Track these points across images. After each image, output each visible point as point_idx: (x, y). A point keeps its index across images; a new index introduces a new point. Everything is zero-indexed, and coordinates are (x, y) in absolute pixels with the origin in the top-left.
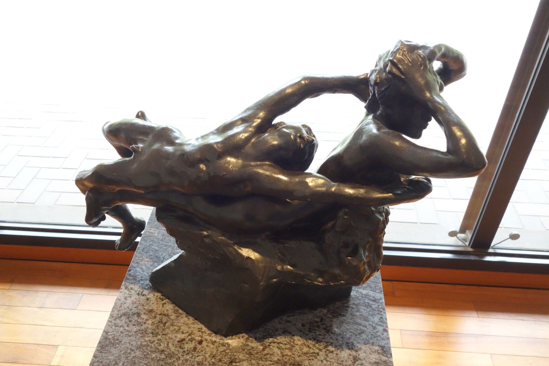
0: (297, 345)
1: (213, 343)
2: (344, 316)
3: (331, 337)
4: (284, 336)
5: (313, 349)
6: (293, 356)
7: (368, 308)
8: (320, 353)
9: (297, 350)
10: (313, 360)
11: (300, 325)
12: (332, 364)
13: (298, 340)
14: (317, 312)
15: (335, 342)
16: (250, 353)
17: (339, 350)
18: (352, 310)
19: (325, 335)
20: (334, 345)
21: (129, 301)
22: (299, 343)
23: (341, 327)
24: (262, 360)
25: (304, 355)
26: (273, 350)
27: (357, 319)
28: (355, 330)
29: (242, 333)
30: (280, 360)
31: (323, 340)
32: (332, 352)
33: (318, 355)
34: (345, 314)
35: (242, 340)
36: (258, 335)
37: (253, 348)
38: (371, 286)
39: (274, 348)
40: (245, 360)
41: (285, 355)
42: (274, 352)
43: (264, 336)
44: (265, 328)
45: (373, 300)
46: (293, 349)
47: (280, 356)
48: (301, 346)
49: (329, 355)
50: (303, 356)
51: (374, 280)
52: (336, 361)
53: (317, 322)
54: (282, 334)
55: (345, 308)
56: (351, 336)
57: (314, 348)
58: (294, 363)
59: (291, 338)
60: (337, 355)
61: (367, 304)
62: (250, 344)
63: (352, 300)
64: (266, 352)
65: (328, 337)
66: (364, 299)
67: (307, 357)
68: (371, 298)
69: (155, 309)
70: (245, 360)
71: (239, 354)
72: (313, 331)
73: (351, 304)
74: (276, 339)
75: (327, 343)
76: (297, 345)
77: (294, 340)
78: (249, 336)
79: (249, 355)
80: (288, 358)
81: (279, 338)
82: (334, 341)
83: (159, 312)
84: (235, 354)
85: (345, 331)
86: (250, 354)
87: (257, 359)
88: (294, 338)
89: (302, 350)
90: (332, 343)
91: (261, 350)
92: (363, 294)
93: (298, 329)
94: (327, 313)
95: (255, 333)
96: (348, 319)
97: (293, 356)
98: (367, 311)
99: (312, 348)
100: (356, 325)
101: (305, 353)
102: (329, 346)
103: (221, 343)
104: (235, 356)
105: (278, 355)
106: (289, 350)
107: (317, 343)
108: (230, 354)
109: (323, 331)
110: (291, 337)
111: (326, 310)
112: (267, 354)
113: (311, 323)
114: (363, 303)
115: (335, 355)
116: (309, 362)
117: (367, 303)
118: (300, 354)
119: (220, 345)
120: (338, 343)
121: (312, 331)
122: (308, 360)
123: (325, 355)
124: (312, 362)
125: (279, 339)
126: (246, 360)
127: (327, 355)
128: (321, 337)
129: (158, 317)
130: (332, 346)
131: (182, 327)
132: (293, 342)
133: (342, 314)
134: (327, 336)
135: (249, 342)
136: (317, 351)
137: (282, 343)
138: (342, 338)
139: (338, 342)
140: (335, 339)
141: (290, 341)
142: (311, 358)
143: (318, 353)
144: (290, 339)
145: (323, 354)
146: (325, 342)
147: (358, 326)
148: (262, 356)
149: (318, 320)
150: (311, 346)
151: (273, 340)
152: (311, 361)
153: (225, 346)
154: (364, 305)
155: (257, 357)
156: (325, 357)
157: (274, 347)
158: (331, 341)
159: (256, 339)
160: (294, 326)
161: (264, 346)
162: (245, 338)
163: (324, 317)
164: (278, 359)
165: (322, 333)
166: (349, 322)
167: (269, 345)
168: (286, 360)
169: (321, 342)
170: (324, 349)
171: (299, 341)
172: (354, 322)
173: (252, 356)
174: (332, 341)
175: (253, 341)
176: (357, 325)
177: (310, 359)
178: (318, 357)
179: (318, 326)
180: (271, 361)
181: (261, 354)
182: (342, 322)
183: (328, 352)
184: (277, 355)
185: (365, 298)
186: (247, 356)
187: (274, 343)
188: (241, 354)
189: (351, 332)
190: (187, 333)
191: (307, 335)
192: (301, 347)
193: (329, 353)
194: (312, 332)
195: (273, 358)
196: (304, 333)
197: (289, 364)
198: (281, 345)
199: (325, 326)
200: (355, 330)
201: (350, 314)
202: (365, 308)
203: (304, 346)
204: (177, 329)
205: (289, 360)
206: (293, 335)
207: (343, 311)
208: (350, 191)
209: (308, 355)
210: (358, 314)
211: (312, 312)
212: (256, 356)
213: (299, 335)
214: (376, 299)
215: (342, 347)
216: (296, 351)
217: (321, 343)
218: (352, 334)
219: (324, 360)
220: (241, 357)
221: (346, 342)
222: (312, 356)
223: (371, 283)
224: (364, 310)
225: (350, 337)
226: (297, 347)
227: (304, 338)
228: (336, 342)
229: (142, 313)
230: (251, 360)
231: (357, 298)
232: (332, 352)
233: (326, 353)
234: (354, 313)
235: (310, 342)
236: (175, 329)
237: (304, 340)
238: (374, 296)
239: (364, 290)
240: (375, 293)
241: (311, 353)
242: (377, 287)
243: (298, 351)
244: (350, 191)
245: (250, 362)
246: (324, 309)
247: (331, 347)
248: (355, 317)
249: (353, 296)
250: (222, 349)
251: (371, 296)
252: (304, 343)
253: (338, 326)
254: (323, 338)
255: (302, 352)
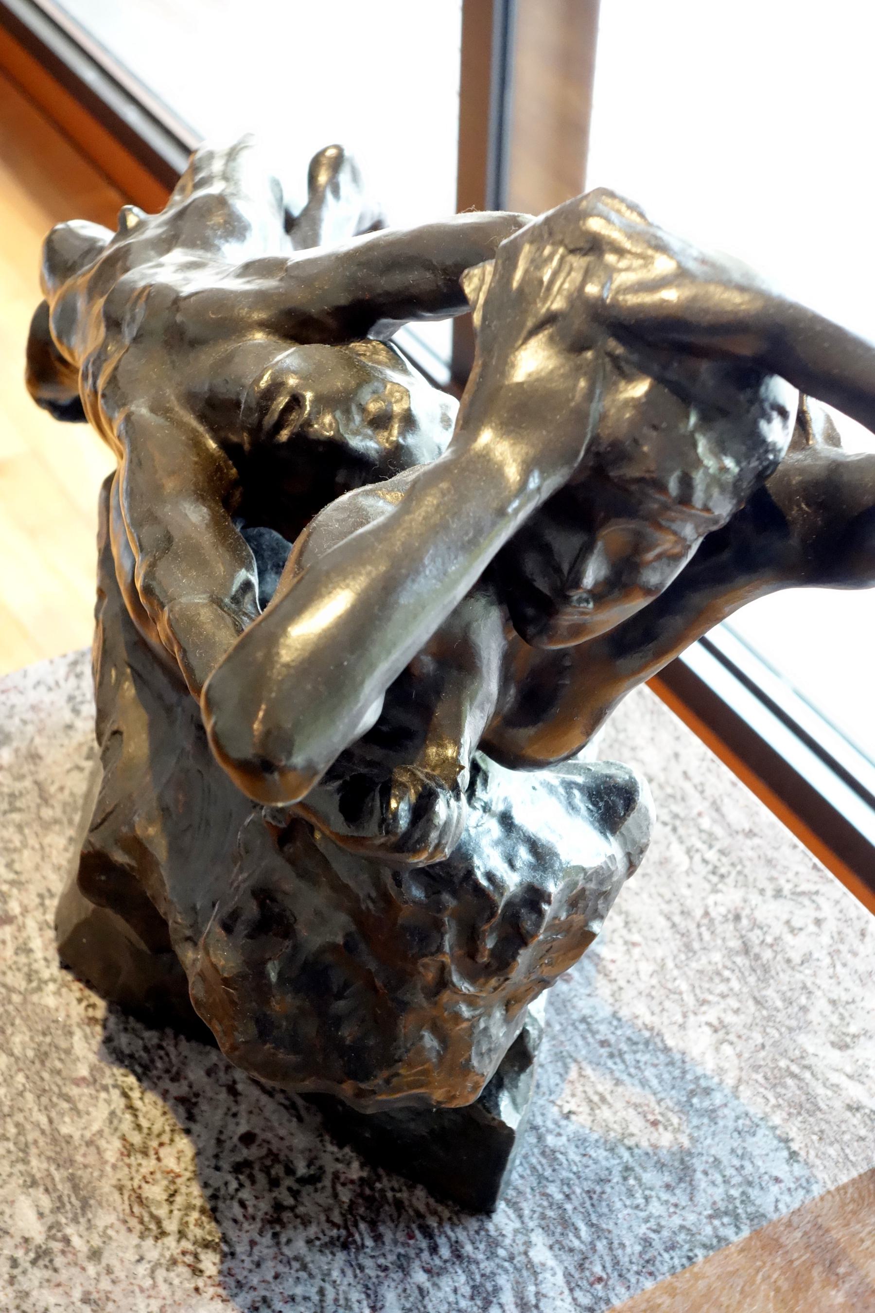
0: (159, 1159)
1: (25, 949)
2: (378, 1238)
3: (257, 1238)
4: (167, 1109)
5: (171, 1211)
6: (108, 1169)
7: (472, 1298)
8: (170, 1241)
9: (137, 1171)
10: (130, 1230)
11: (243, 1129)
12: (147, 1293)
13: (180, 1152)
14: (332, 1153)
15: (243, 1261)
16: (46, 1054)
17: (220, 1291)
18: (421, 1250)
19: (254, 1218)
20: (229, 1263)
21: (41, 696)
22: (170, 1162)
23: (321, 1251)
24: (39, 1097)
25: (133, 1198)
26: (95, 1106)
27: (393, 1285)
28: (342, 1302)
29: (103, 997)
30: (68, 1143)
31: (228, 1224)
32: (197, 1272)
33: (157, 1239)
34: (388, 1237)
35: (78, 1011)
36: (123, 1041)
37: (68, 1052)
38: (587, 1265)
39: (102, 1104)
40: (12, 1054)
41: (98, 1148)
42: (88, 1113)
43: (131, 1056)
44: (164, 1044)
45: (522, 1299)
46: (132, 1158)
47: (82, 1136)
48: (163, 1172)
49: (181, 1269)
50: (126, 1197)
51: (631, 1262)
52: (169, 1301)
53: (290, 1171)
54: (172, 1101)
55: (414, 1226)
56: (306, 1299)
57: (176, 1212)
58: (81, 1185)
59: (172, 1131)
60: (194, 1294)
61: (490, 1289)
62: (78, 1035)
63: (472, 1233)
64: (74, 1091)
65: (247, 1231)
66: (506, 1271)
67: (128, 1211)
68: (532, 1289)
69: (48, 760)
70: (12, 1054)
71: (25, 1029)
72: (241, 1177)
73: (448, 1238)
74: (143, 1093)
75: (225, 1239)
76: (159, 1159)
77: (172, 1141)
78: (105, 1021)
79: (36, 1055)
80: (92, 1159)
81: (150, 1097)
82: (244, 1257)
83: (41, 776)
84: (18, 1021)
85: (315, 1271)
86: (42, 1057)
87: (35, 1083)
88: (177, 1138)
89: (147, 1182)
90: (233, 1254)
91: (75, 1075)
92: (526, 1253)
93: (221, 1132)
94: (352, 1182)
95: (126, 1030)
96: (373, 1257)
97: (108, 1169)
98: (457, 1303)
99: (176, 1206)
100: (363, 1296)
101: (139, 1197)
102: (215, 1250)
103: (35, 966)
104: (13, 1025)
105: (85, 1128)
106: (124, 1147)
107: (203, 1211)
108: (10, 1008)
109: (265, 1206)
110: (177, 1128)
111: (364, 1174)
112: (68, 1099)
113: (273, 1156)
114: (483, 1275)
115: (193, 1286)
116: (112, 1226)
117: (495, 1286)
118: (128, 1184)
119: (26, 969)
120: (245, 1273)
121: (242, 1173)
122: (119, 1220)
123: (172, 1255)
124: (117, 1232)
125: (146, 1101)
126: (12, 1059)
127: (174, 1262)
128: (237, 1211)
129: (28, 783)
130: (222, 1262)
131: (26, 853)
132: (161, 1144)
133: (382, 1229)
134: (251, 1229)
135: (83, 1030)
136: (171, 1226)
137: (136, 1116)
138: (276, 1277)
139: (250, 1271)
140: (256, 1258)
141: (159, 1135)
142: (133, 1222)
143: (163, 1234)
144: (167, 1128)
145: (168, 1249)
146: (223, 1234)
147: (365, 1303)
148: (56, 1089)
149: (302, 1169)
150: (179, 1200)
151: (131, 1089)
152: (123, 1229)
153: (30, 981)
154: (474, 1280)
155: (42, 1079)
156: (163, 1261)
157: (108, 1102)
158: (241, 1249)
159: (108, 1040)
160: (226, 1114)
161: (92, 1075)
162: (91, 1012)
163: (327, 1182)
164: (71, 1137)
165: (254, 1206)
166: (361, 1268)
167: (105, 1088)
168: (79, 1158)
169: (217, 1221)
170: (194, 1244)
171: (178, 1158)
172: (374, 1280)
173: (38, 1065)
174: (242, 1253)
175: (94, 1037)
176: (368, 1296)
177: (125, 1222)
178: (150, 1241)
179: (274, 1183)
180: (51, 1121)
181: (60, 1082)
182: (345, 1247)
183: (189, 1259)
184: (82, 1125)
185: (511, 1270)
186: (30, 1054)
187: (125, 1095)
188: (28, 1034)
189: (321, 1292)
190: (17, 873)
191: (217, 1168)
192: (158, 1176)
193: (189, 1266)
194: (237, 1179)
195: (64, 1122)
196: (216, 1156)
197: (72, 1175)
198: (128, 1117)
199: (289, 1201)
200: (336, 1300)
201: (399, 1256)
202: (467, 1290)
203: (165, 1183)
204: (11, 846)
205: (86, 1166)
206: (188, 1132)
207: (396, 1226)
208: (261, 714)
209: (137, 1209)
210: (420, 1277)
211: (321, 1135)
212: (46, 1075)
213: (201, 1146)
214: (537, 1306)
215: (236, 1295)
216: (133, 1169)
217: (213, 1224)
218: (316, 1298)
219: (149, 1262)
220: (17, 1039)
221: (267, 1294)
222: (142, 1222)
223: (608, 1259)
224: (455, 1291)
225: (298, 1299)
226: (149, 1164)
227: (196, 1165)
228: (248, 1264)
229: (15, 744)
230: (20, 1070)
231: (493, 1244)
232: (197, 1272)
233: (180, 1258)
234: (416, 1265)
235: (196, 1189)
236: (10, 841)
237: (191, 1168)
238: (545, 1296)
239: (551, 1247)
240: (567, 1292)
241: (153, 1216)
242: (599, 1287)
243: (134, 1174)
244: (261, 714)
245: (13, 1073)
246: (362, 1166)
247: (216, 1258)
248: (398, 1276)
249: (490, 1227)
250: (17, 980)
251: (536, 1285)
252: (178, 1176)
253: (318, 1239)
254: (235, 1221)
255: (140, 1187)
